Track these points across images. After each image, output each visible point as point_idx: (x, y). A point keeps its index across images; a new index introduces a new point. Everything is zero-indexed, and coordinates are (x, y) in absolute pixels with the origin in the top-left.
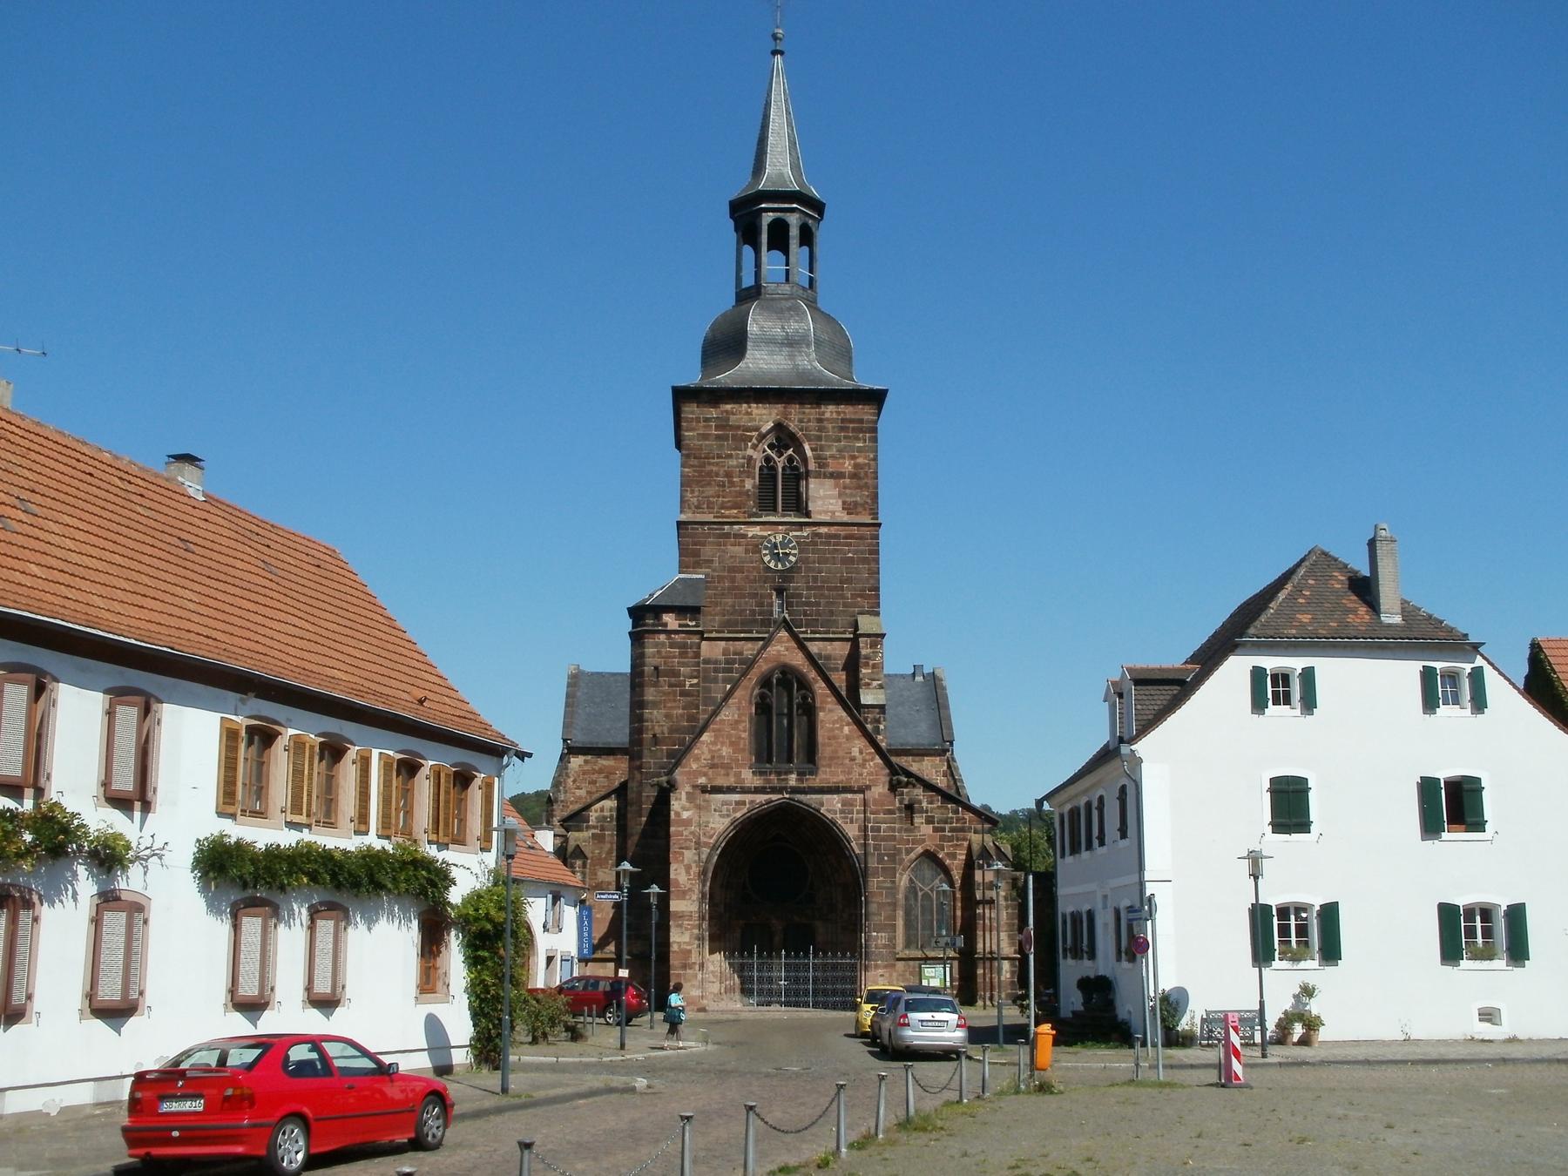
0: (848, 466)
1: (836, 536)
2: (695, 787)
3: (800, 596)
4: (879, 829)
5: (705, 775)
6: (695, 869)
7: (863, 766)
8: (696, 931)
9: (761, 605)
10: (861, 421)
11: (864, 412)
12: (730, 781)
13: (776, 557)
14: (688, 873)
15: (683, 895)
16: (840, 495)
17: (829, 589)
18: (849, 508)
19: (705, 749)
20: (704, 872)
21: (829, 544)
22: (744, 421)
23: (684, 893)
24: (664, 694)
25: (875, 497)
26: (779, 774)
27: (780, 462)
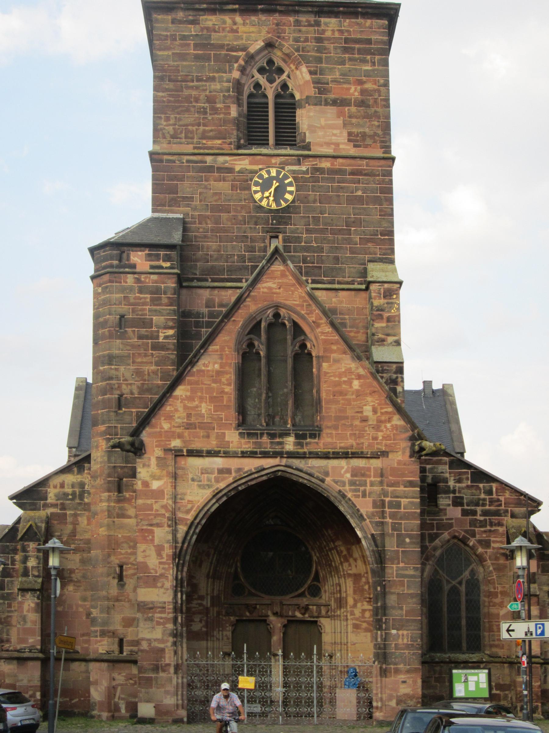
0: (354, 92)
1: (340, 172)
2: (167, 450)
3: (298, 240)
4: (398, 505)
5: (180, 436)
6: (168, 551)
7: (377, 428)
8: (170, 626)
9: (252, 249)
10: (369, 41)
11: (372, 27)
12: (213, 444)
14: (159, 555)
15: (152, 581)
16: (345, 125)
17: (333, 232)
18: (355, 139)
19: (179, 405)
20: (178, 555)
21: (333, 180)
22: (229, 39)
23: (155, 579)
24: (133, 346)
25: (386, 128)
26: (272, 436)
27: (270, 91)
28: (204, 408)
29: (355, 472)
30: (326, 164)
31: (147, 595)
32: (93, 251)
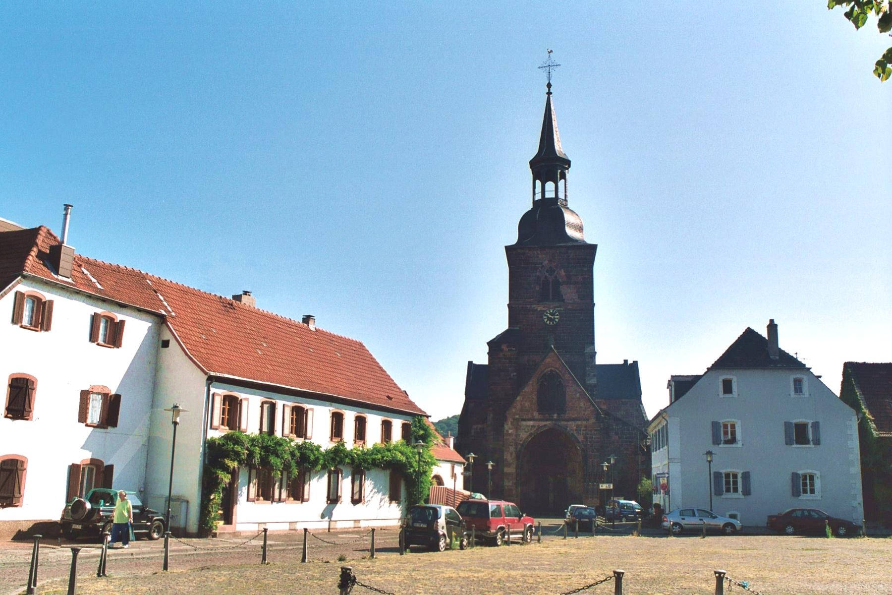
2: (514, 419)
6: (514, 454)
13: (549, 319)
15: (509, 465)
29: (578, 426)
30: (570, 307)
31: (506, 470)
32: (488, 343)
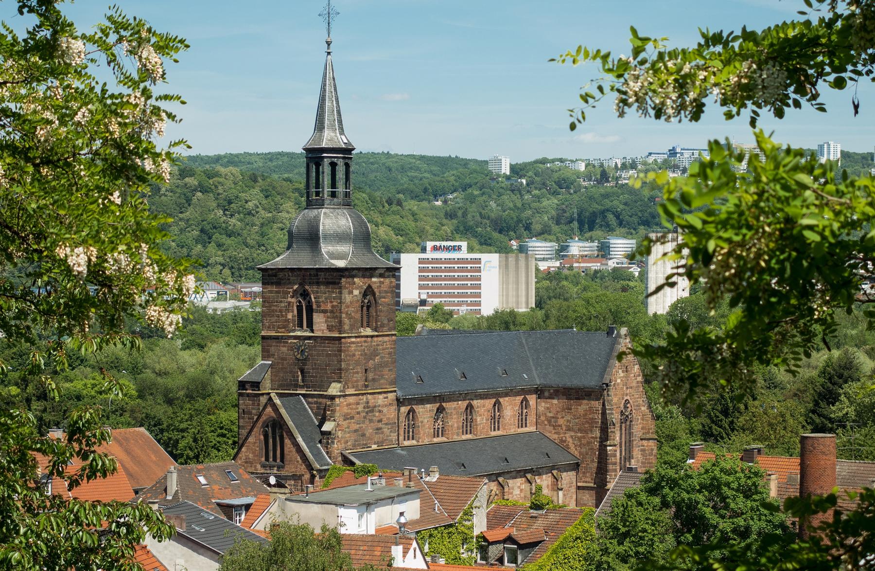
0: (329, 307)
28: (251, 456)
